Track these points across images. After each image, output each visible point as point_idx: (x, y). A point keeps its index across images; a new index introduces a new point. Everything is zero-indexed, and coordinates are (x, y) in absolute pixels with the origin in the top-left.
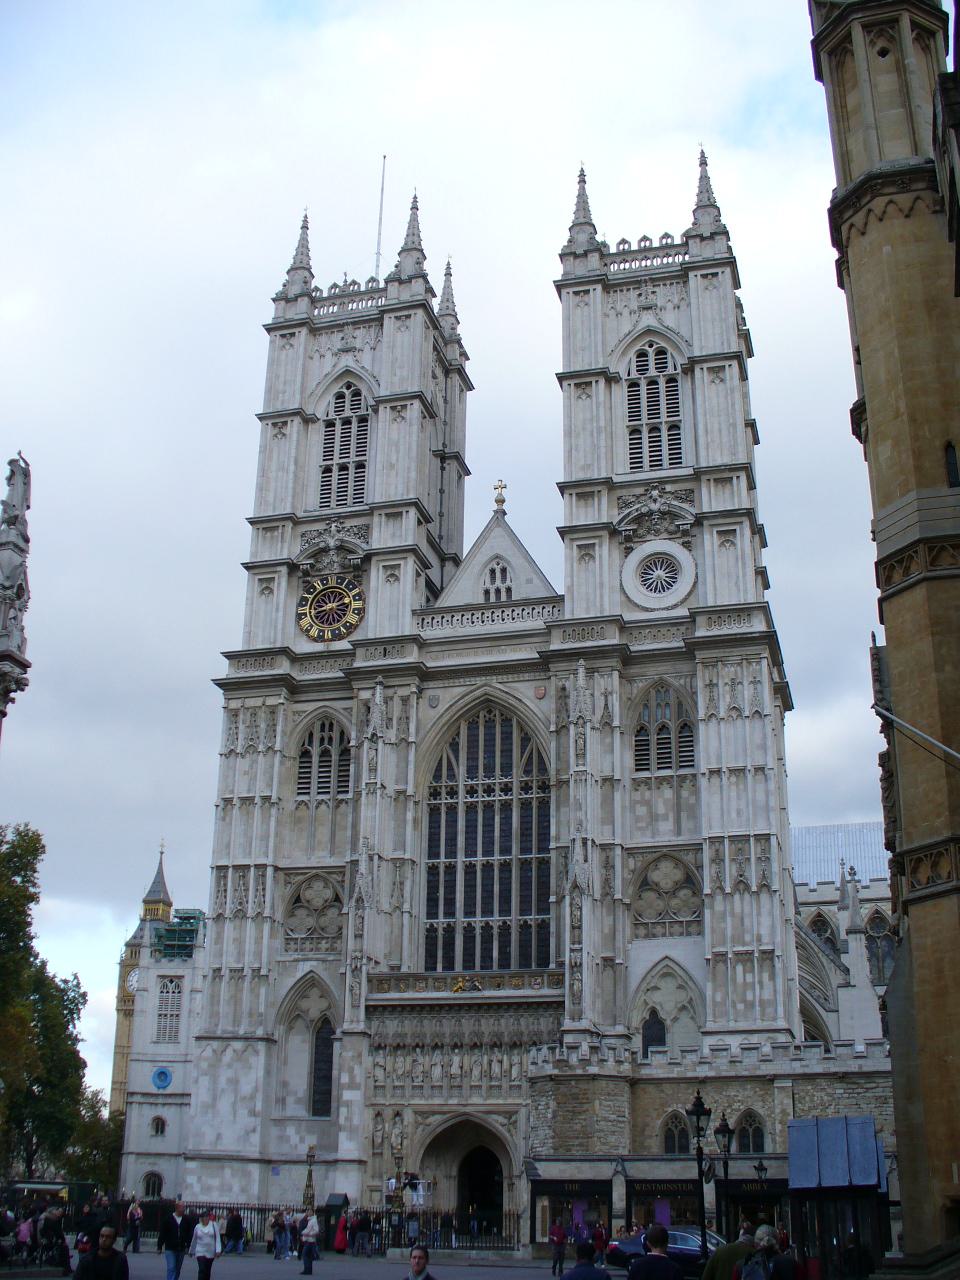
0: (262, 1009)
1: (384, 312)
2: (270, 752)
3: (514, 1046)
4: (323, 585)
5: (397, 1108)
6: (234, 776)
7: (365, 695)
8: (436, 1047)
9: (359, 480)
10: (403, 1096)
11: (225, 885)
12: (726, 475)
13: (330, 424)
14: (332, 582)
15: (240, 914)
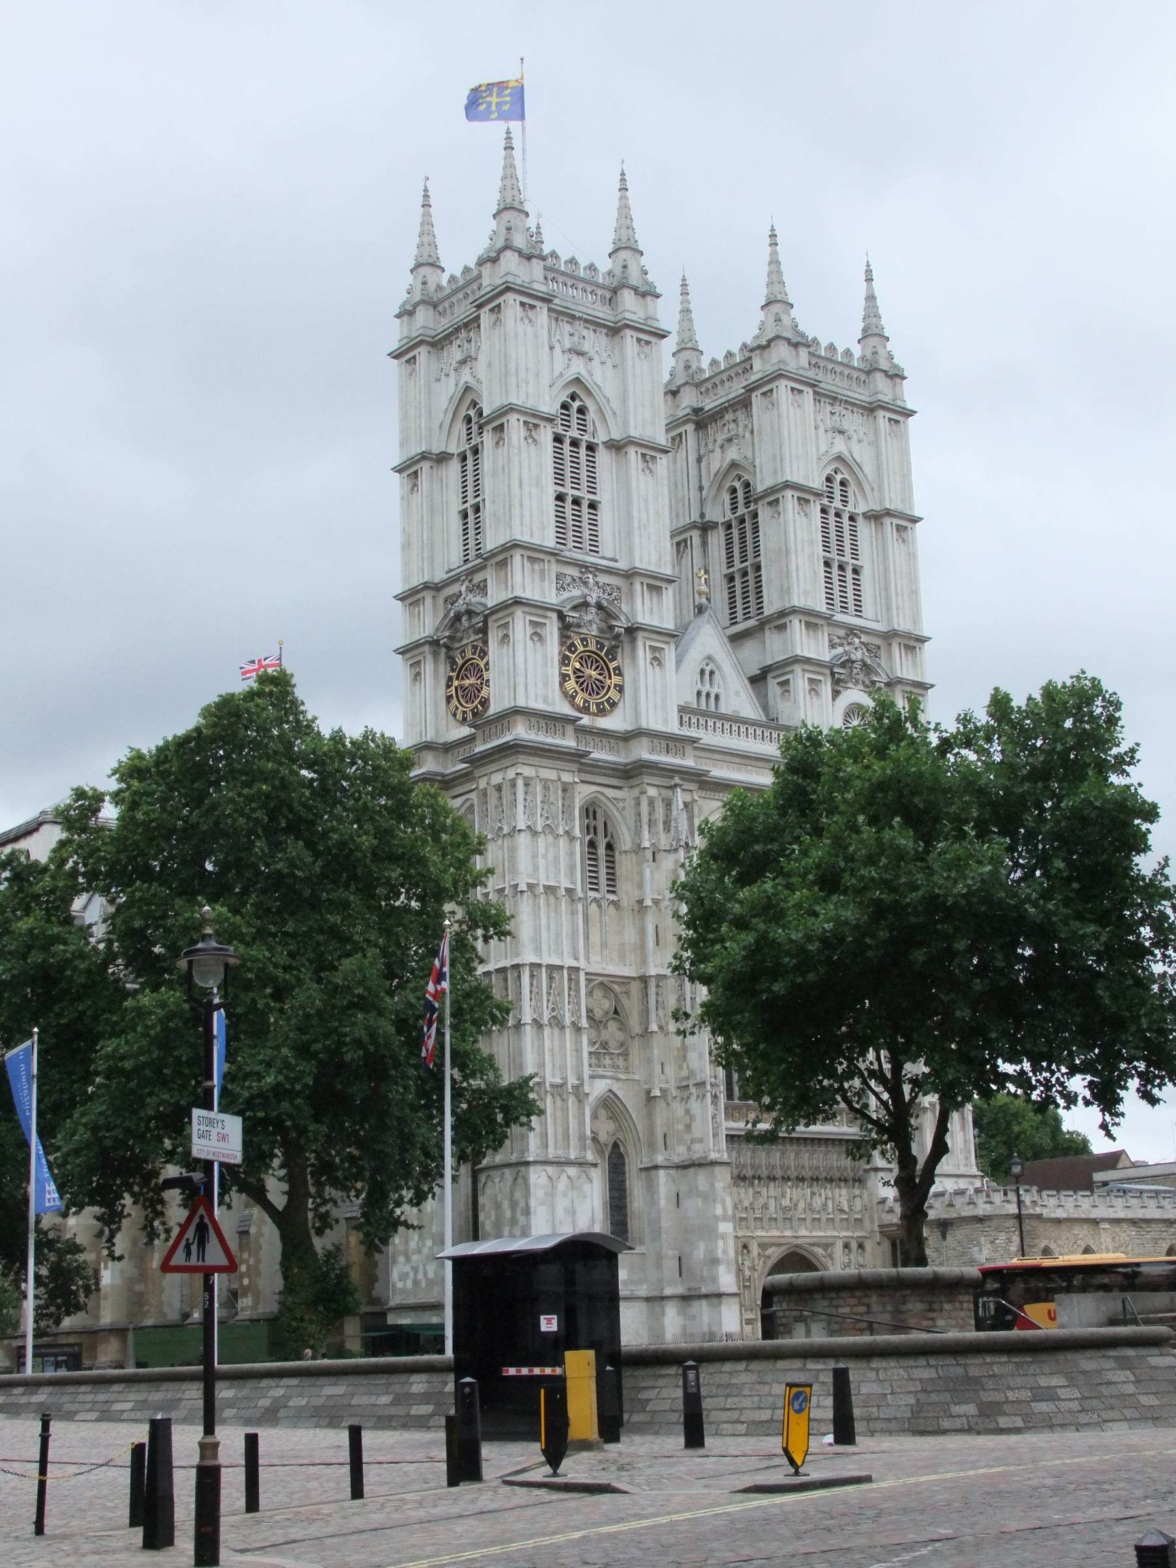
0: (588, 1133)
1: (627, 326)
2: (566, 837)
3: (831, 1180)
4: (584, 646)
5: (744, 1240)
6: (535, 856)
7: (652, 792)
8: (774, 1179)
9: (594, 523)
10: (748, 1228)
11: (540, 987)
12: (912, 643)
13: (558, 439)
14: (592, 647)
15: (557, 1022)
